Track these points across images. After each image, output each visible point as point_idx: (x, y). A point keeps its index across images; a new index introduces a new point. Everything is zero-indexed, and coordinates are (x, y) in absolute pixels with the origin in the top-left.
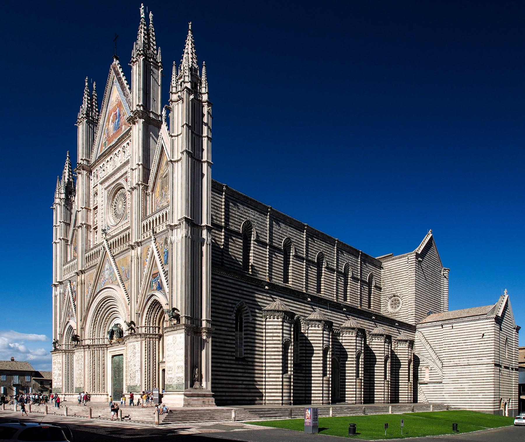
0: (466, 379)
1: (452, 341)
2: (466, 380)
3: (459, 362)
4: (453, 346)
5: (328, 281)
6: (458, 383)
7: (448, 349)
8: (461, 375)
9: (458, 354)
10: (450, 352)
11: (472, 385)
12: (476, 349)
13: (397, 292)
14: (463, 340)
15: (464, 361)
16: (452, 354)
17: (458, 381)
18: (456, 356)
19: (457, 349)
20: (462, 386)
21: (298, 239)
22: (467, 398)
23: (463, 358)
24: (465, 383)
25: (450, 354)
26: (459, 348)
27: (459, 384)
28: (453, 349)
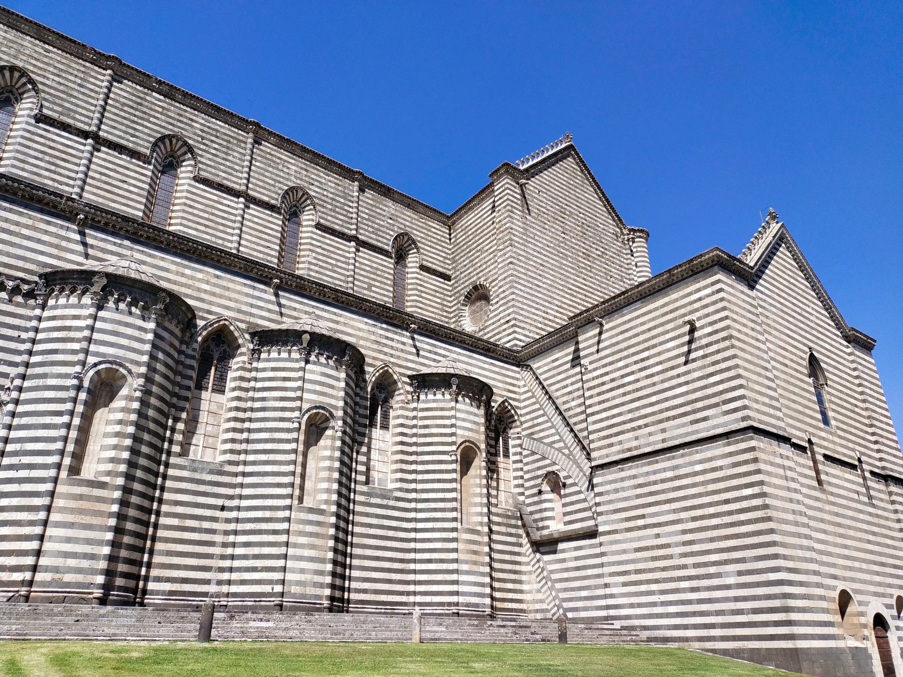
0: (666, 507)
1: (607, 374)
2: (669, 512)
3: (635, 443)
4: (612, 390)
5: (206, 215)
6: (645, 527)
7: (600, 403)
8: (651, 494)
9: (630, 411)
10: (605, 410)
11: (691, 531)
12: (680, 385)
13: (480, 275)
14: (636, 363)
15: (650, 434)
16: (614, 416)
17: (643, 517)
18: (624, 423)
19: (624, 394)
20: (658, 536)
21: (70, 84)
22: (684, 590)
23: (646, 426)
24: (667, 524)
25: (607, 418)
26: (629, 393)
27: (649, 532)
28: (614, 398)
